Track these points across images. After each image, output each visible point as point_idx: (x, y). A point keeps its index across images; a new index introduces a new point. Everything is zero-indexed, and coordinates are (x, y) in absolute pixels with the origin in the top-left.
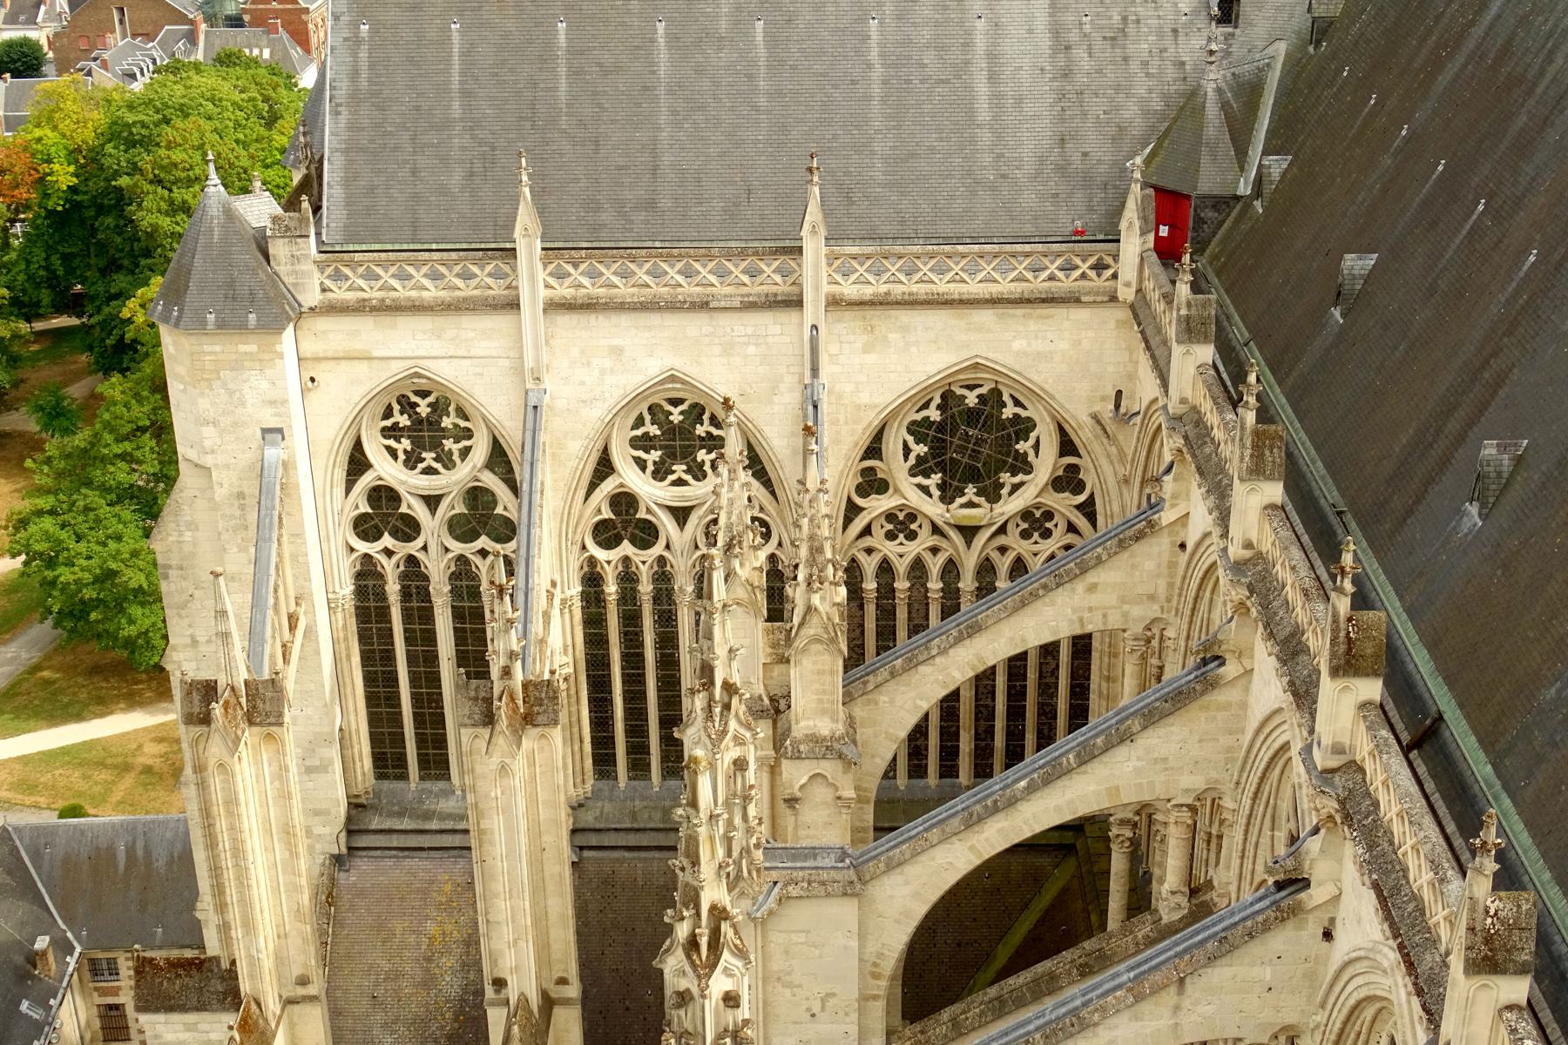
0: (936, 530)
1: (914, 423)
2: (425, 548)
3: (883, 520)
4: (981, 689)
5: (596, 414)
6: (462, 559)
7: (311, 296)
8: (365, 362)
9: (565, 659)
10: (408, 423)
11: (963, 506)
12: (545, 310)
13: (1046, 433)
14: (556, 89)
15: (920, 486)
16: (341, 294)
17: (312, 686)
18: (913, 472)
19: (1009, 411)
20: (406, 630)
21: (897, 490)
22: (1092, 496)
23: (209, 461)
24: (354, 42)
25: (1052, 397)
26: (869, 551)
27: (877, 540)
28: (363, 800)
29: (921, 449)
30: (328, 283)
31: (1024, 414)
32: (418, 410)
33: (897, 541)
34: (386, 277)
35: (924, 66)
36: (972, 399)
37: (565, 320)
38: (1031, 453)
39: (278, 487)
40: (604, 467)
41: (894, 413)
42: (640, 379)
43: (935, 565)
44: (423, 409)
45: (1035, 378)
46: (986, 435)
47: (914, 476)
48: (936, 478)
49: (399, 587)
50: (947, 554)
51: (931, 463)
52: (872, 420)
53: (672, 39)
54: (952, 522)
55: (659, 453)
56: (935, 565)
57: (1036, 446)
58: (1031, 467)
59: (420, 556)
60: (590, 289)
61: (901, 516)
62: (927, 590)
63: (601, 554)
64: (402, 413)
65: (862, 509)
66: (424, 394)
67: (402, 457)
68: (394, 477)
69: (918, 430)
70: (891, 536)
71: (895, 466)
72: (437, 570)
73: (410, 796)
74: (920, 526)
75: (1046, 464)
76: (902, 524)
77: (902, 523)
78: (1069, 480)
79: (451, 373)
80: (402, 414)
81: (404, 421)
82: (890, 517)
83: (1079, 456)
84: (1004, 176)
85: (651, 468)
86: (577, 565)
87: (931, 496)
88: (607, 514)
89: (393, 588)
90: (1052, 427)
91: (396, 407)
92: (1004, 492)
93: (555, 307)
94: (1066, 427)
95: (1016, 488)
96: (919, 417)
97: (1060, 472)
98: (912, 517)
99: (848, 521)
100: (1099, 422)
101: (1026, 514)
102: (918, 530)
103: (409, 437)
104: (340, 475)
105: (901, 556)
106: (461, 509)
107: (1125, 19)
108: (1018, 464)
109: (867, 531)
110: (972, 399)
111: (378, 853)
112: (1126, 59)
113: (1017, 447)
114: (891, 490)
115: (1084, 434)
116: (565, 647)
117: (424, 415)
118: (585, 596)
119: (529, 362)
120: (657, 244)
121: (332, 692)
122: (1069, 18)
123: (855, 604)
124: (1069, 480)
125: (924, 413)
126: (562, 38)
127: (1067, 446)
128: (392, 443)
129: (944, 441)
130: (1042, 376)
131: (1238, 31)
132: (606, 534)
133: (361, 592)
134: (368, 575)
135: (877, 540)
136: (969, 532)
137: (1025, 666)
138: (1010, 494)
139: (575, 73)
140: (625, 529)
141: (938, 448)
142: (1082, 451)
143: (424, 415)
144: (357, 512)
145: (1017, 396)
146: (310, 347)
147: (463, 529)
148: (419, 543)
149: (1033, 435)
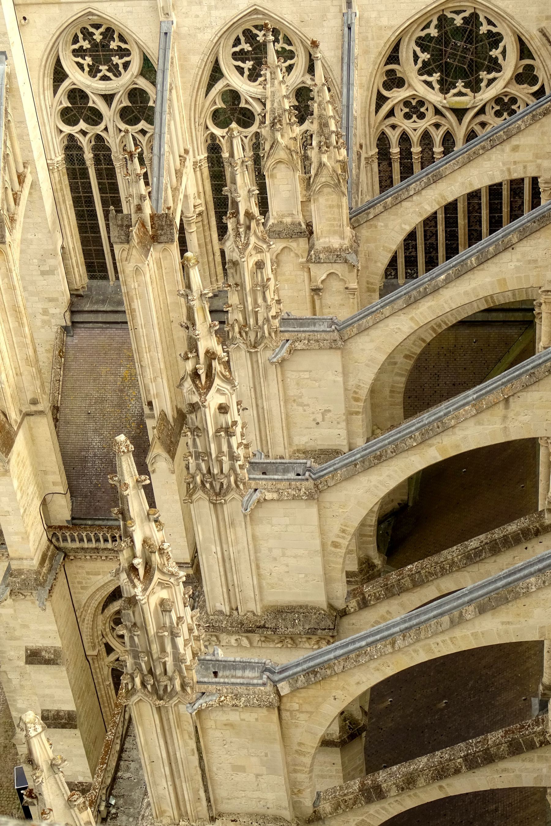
0: (437, 112)
1: (420, 38)
4: (472, 219)
9: (198, 201)
10: (89, 46)
11: (455, 95)
17: (40, 220)
18: (421, 72)
20: (99, 184)
21: (410, 85)
22: (543, 87)
27: (398, 119)
28: (81, 292)
29: (425, 56)
32: (94, 37)
33: (412, 120)
39: (4, 91)
41: (405, 31)
42: (234, 12)
44: (98, 37)
46: (469, 46)
47: (421, 75)
48: (436, 76)
50: (446, 128)
51: (433, 66)
54: (447, 106)
55: (252, 63)
58: (501, 67)
61: (414, 103)
62: (433, 153)
65: (387, 99)
66: (97, 26)
67: (87, 69)
68: (82, 83)
70: (407, 116)
73: (110, 290)
77: (414, 107)
80: (84, 40)
81: (86, 45)
82: (407, 103)
83: (533, 59)
85: (247, 73)
86: (203, 139)
87: (433, 88)
90: (513, 39)
91: (81, 36)
92: (483, 85)
94: (523, 38)
95: (490, 82)
96: (423, 34)
98: (421, 103)
99: (378, 107)
100: (544, 35)
101: (498, 100)
102: (425, 112)
103: (90, 56)
105: (415, 130)
108: (492, 65)
109: (391, 113)
111: (91, 325)
114: (406, 85)
116: (199, 193)
117: (98, 41)
118: (210, 159)
121: (54, 223)
123: (385, 163)
125: (426, 31)
128: (79, 60)
129: (441, 50)
135: (398, 119)
136: (460, 113)
137: (501, 203)
140: (233, 114)
142: (535, 56)
143: (98, 41)
144: (61, 106)
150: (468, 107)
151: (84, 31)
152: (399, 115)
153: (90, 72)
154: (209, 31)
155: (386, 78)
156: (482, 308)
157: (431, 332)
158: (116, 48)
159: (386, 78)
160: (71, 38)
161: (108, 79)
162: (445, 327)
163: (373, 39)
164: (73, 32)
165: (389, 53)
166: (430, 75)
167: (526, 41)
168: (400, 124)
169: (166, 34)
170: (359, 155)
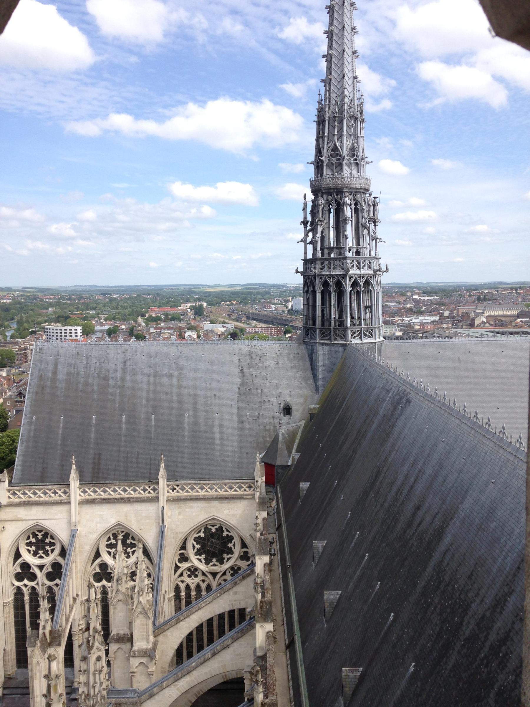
0: (204, 574)
1: (196, 538)
2: (38, 584)
5: (94, 537)
8: (21, 522)
12: (79, 504)
13: (237, 540)
15: (198, 559)
18: (196, 554)
21: (191, 561)
25: (237, 529)
26: (183, 582)
27: (185, 578)
29: (198, 546)
30: (11, 496)
31: (230, 534)
32: (38, 537)
33: (191, 578)
36: (214, 530)
38: (233, 547)
40: (98, 555)
42: (109, 525)
43: (203, 586)
44: (40, 536)
48: (203, 556)
49: (28, 598)
52: (181, 537)
53: (128, 420)
54: (208, 571)
56: (203, 586)
57: (234, 545)
59: (36, 587)
61: (192, 569)
64: (33, 538)
65: (180, 567)
67: (32, 552)
70: (189, 576)
72: (42, 591)
74: (199, 573)
75: (237, 551)
76: (193, 572)
77: (193, 572)
78: (245, 557)
79: (49, 525)
80: (33, 538)
81: (33, 540)
82: (189, 569)
84: (223, 460)
88: (98, 570)
89: (27, 598)
91: (31, 536)
92: (225, 561)
95: (229, 559)
96: (197, 536)
97: (242, 554)
98: (196, 569)
99: (176, 571)
101: (232, 568)
102: (198, 574)
103: (35, 546)
104: (12, 559)
105: (193, 583)
106: (50, 570)
107: (259, 414)
108: (229, 551)
109: (181, 575)
112: (259, 425)
113: (228, 545)
114: (189, 561)
115: (248, 541)
117: (40, 538)
119: (73, 520)
120: (117, 482)
122: (243, 414)
123: (177, 601)
124: (245, 557)
125: (199, 534)
126: (94, 421)
127: (244, 545)
128: (29, 548)
129: (205, 543)
131: (292, 417)
135: (185, 578)
136: (214, 575)
138: (227, 561)
141: (203, 546)
143: (40, 538)
145: (227, 528)
147: (50, 576)
148: (36, 582)
149: (233, 541)
150: (218, 572)
152: (185, 575)
154: (95, 534)
155: (179, 557)
156: (221, 682)
157: (194, 696)
158: (48, 542)
159: (179, 557)
160: (26, 537)
163: (174, 538)
164: (28, 534)
165: (181, 545)
166: (200, 555)
167: (244, 540)
168: (185, 580)
169: (74, 535)
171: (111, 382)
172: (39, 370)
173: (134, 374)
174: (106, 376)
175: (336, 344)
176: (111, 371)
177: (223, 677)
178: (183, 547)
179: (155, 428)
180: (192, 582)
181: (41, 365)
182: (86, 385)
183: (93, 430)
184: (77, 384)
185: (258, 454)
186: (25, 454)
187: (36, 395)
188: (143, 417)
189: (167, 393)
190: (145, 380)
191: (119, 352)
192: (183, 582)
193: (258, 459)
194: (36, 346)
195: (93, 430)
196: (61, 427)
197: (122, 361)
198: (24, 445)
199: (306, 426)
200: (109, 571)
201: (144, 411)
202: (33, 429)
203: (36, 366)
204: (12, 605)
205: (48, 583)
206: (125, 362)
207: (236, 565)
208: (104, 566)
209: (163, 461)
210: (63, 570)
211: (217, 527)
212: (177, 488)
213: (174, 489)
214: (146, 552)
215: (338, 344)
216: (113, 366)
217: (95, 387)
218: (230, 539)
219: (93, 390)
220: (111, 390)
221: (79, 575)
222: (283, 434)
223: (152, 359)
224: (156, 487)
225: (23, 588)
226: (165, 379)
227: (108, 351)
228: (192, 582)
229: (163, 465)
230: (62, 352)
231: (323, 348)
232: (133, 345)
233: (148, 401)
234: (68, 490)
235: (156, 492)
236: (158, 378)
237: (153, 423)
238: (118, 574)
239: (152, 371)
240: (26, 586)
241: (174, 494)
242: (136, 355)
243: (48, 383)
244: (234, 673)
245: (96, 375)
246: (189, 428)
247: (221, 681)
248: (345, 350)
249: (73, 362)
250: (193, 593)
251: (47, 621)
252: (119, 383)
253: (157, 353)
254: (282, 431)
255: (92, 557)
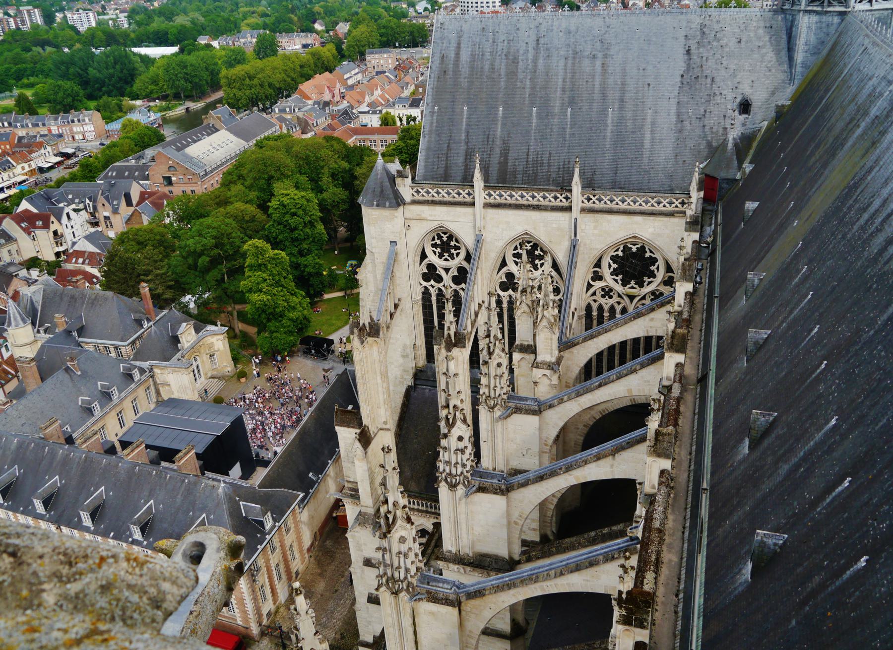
0: (619, 296)
1: (613, 256)
3: (600, 290)
5: (501, 244)
6: (455, 291)
7: (408, 198)
11: (630, 288)
13: (661, 263)
14: (496, 131)
16: (418, 197)
18: (612, 274)
19: (648, 255)
23: (374, 251)
24: (432, 113)
25: (663, 250)
26: (595, 301)
29: (615, 266)
31: (653, 256)
34: (433, 192)
35: (627, 126)
36: (634, 249)
37: (492, 212)
38: (656, 271)
40: (504, 264)
43: (618, 308)
44: (445, 239)
45: (657, 243)
48: (620, 277)
56: (618, 308)
57: (658, 268)
59: (443, 288)
60: (499, 200)
61: (607, 289)
63: (501, 293)
67: (437, 254)
69: (614, 259)
70: (603, 296)
71: (606, 272)
72: (448, 293)
75: (661, 275)
76: (607, 292)
79: (454, 228)
81: (439, 242)
82: (603, 290)
89: (434, 299)
91: (436, 237)
92: (645, 284)
93: (488, 206)
95: (649, 283)
96: (614, 254)
97: (666, 279)
98: (611, 290)
99: (588, 290)
101: (653, 293)
104: (418, 259)
106: (456, 273)
107: (705, 111)
109: (594, 294)
110: (634, 249)
112: (704, 126)
115: (674, 266)
119: (478, 225)
122: (684, 110)
125: (617, 253)
126: (500, 113)
127: (669, 269)
128: (434, 249)
130: (659, 242)
132: (504, 287)
133: (424, 299)
134: (426, 293)
136: (632, 298)
138: (648, 285)
139: (504, 125)
146: (408, 215)
147: (457, 280)
148: (442, 284)
149: (657, 264)
151: (438, 235)
152: (599, 294)
153: (439, 256)
161: (448, 260)
162: (607, 412)
166: (617, 276)
170: (573, 314)
171: (521, 65)
172: (441, 50)
173: (548, 56)
174: (515, 58)
175: (830, 12)
176: (521, 52)
177: (631, 400)
178: (598, 264)
179: (571, 126)
180: (607, 303)
181: (443, 43)
182: (493, 69)
183: (499, 124)
184: (482, 68)
185: (697, 164)
186: (428, 149)
187: (438, 81)
188: (557, 110)
189: (587, 81)
190: (562, 63)
191: (532, 26)
192: (595, 301)
193: (697, 169)
194: (437, 20)
195: (499, 124)
196: (465, 120)
197: (535, 38)
198: (427, 139)
199: (768, 128)
200: (516, 281)
201: (558, 103)
202: (435, 121)
203: (438, 44)
204: (420, 303)
205: (454, 287)
206: (538, 40)
207: (658, 290)
208: (510, 276)
209: (578, 165)
210: (468, 276)
211: (639, 246)
212: (594, 199)
213: (589, 199)
214: (555, 266)
215: (834, 12)
216: (524, 45)
217: (503, 72)
218: (654, 261)
219: (500, 75)
220: (521, 76)
221: (485, 282)
222: (734, 139)
223: (571, 35)
224: (569, 196)
225: (430, 288)
226: (586, 62)
227: (519, 25)
228: (607, 303)
229: (577, 171)
230: (466, 27)
231: (809, 18)
232: (548, 17)
233: (564, 90)
234: (471, 192)
235: (569, 201)
236: (578, 60)
237: (569, 119)
238: (523, 285)
239: (571, 52)
240: (433, 287)
241: (589, 205)
242: (552, 30)
243: (451, 66)
244: (644, 398)
245: (503, 56)
246: (613, 126)
247: (629, 403)
248: (842, 21)
249: (478, 40)
250: (606, 314)
251: (451, 323)
252: (530, 67)
253: (578, 28)
254: (733, 135)
255: (498, 266)
